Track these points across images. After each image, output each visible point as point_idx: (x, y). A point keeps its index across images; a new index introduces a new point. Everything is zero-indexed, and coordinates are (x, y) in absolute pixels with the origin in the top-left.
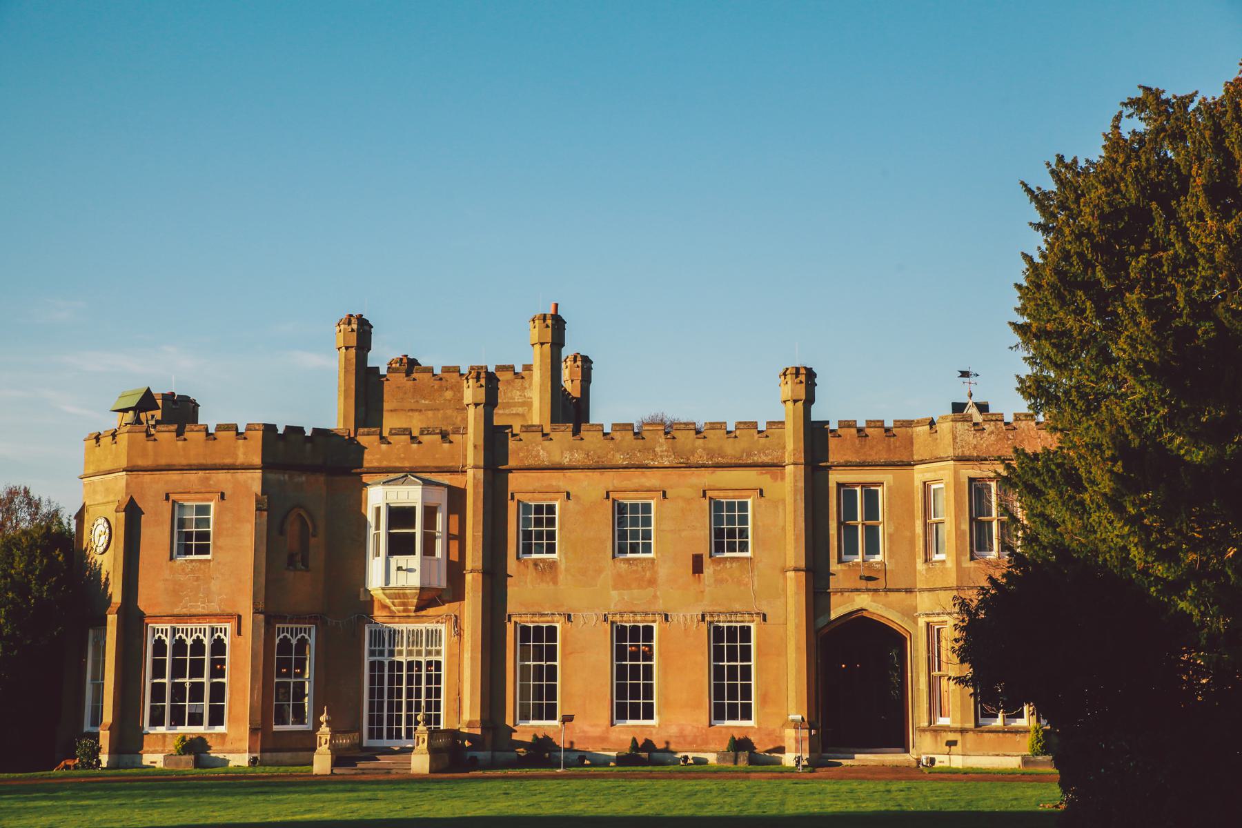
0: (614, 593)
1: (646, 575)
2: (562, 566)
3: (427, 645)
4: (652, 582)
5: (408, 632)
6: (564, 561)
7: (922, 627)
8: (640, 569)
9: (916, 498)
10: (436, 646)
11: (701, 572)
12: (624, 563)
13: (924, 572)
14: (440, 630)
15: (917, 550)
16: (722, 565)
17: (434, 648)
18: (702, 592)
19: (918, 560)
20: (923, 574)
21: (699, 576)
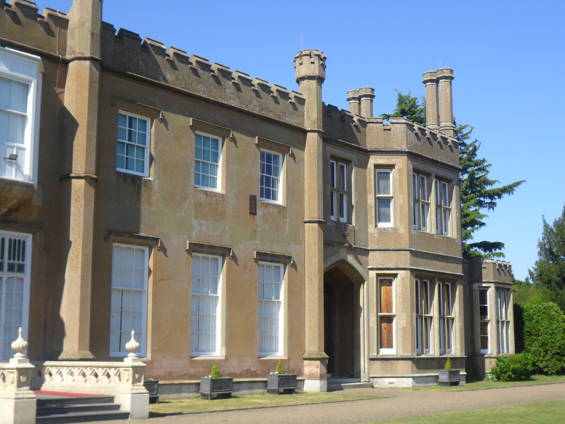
0: (195, 222)
1: (218, 208)
2: (156, 187)
3: (9, 259)
4: (222, 216)
5: (10, 240)
6: (157, 182)
7: (373, 278)
8: (214, 202)
9: (368, 177)
10: (18, 260)
11: (255, 214)
12: (203, 194)
13: (376, 235)
14: (24, 242)
15: (369, 217)
16: (267, 209)
17: (16, 262)
18: (255, 231)
19: (370, 226)
20: (374, 237)
21: (254, 217)
